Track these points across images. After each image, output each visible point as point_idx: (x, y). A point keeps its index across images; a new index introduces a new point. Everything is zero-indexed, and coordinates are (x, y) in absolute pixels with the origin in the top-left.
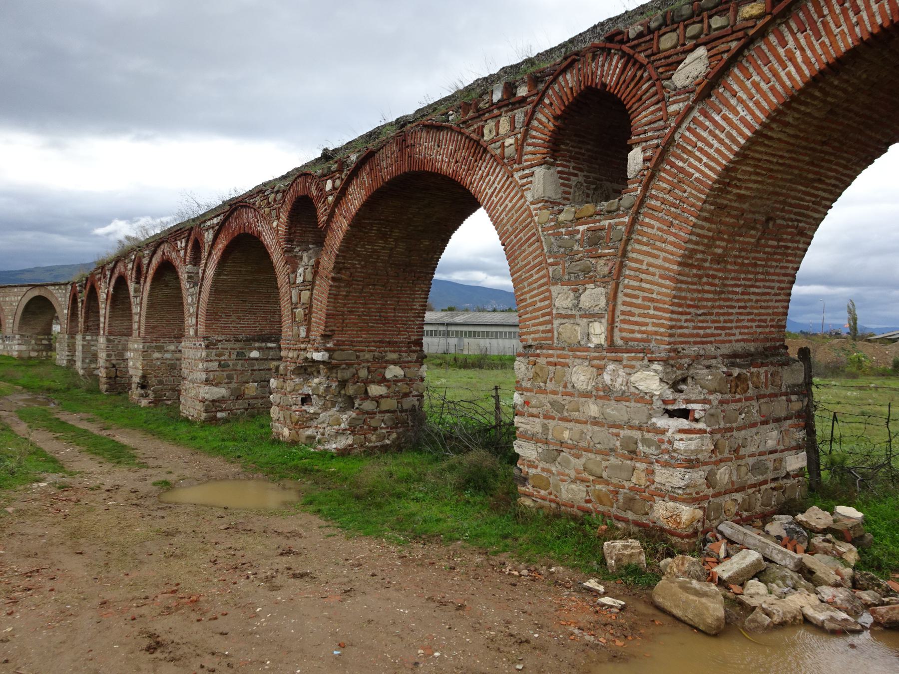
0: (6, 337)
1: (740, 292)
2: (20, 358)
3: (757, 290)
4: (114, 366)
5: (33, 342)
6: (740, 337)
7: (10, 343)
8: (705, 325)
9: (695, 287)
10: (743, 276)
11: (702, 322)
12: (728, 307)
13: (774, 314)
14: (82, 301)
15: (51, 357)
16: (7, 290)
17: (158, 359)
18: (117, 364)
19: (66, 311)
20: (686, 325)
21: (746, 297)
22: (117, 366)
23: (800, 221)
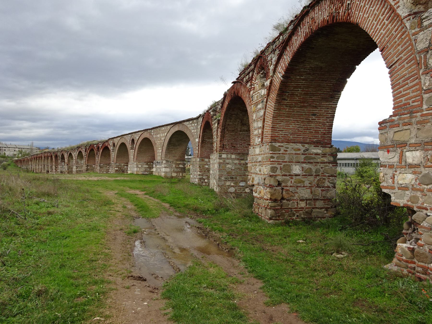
0: (157, 162)
2: (166, 177)
4: (279, 184)
5: (174, 166)
7: (160, 166)
14: (219, 120)
15: (185, 177)
16: (158, 129)
18: (283, 181)
19: (197, 140)
22: (283, 184)
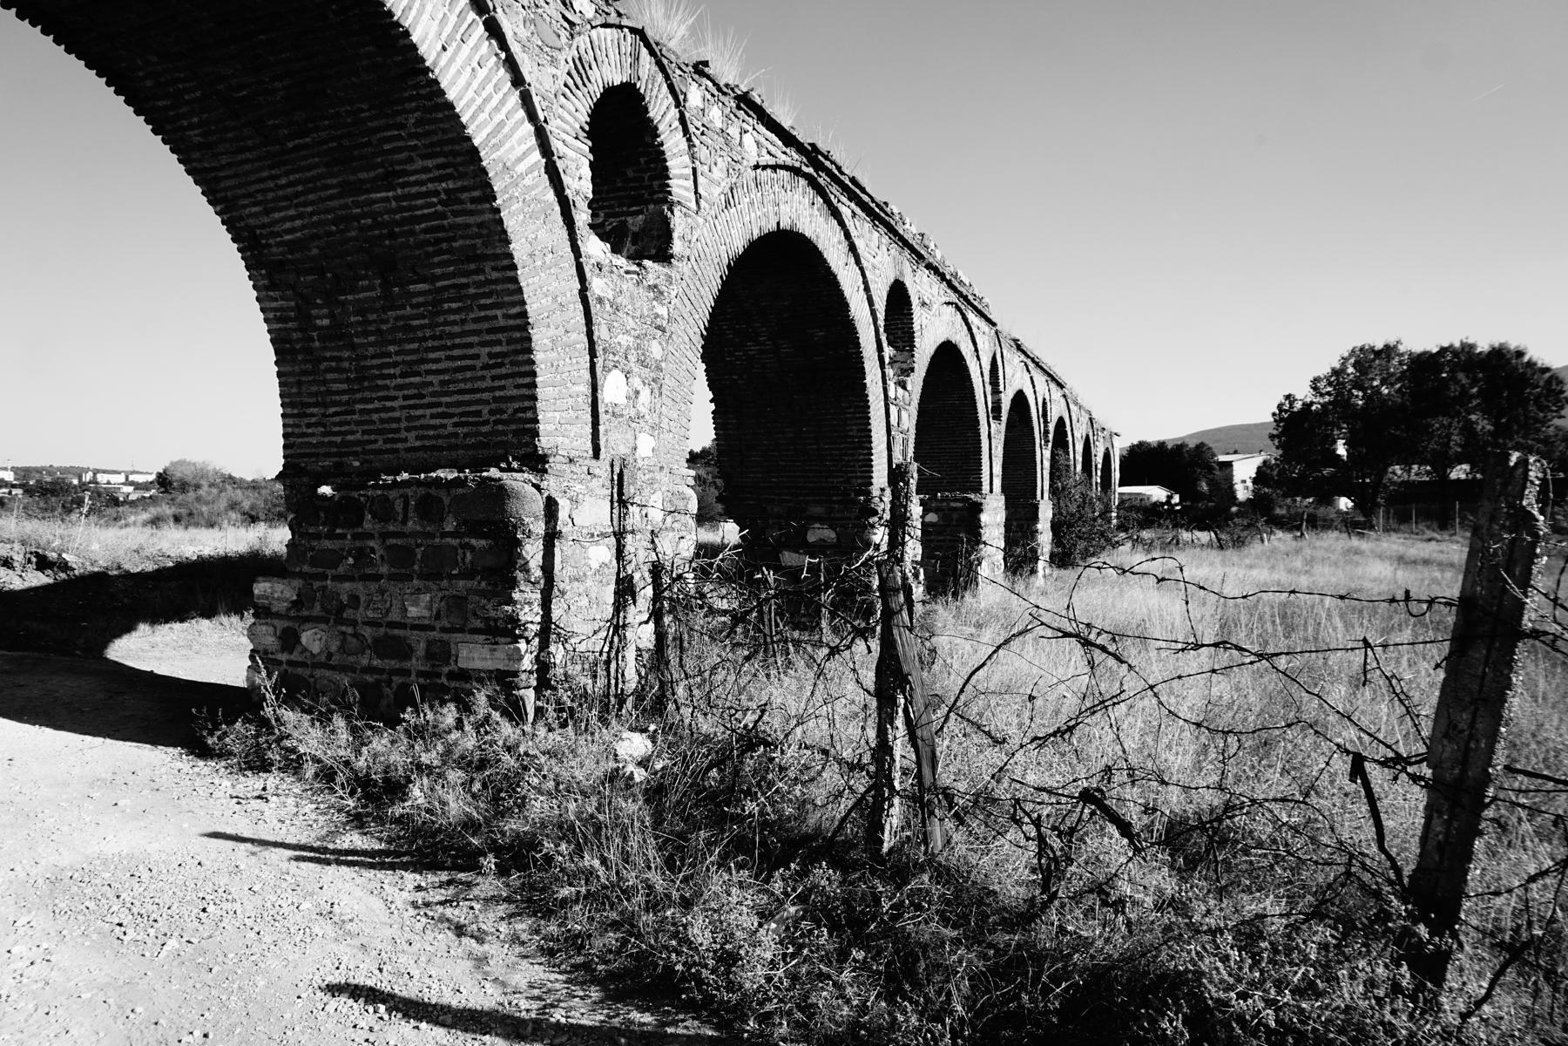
1: (398, 374)
3: (434, 367)
6: (418, 443)
8: (343, 429)
9: (310, 378)
10: (392, 349)
11: (341, 424)
12: (380, 399)
13: (495, 399)
20: (310, 431)
21: (417, 380)
23: (454, 239)
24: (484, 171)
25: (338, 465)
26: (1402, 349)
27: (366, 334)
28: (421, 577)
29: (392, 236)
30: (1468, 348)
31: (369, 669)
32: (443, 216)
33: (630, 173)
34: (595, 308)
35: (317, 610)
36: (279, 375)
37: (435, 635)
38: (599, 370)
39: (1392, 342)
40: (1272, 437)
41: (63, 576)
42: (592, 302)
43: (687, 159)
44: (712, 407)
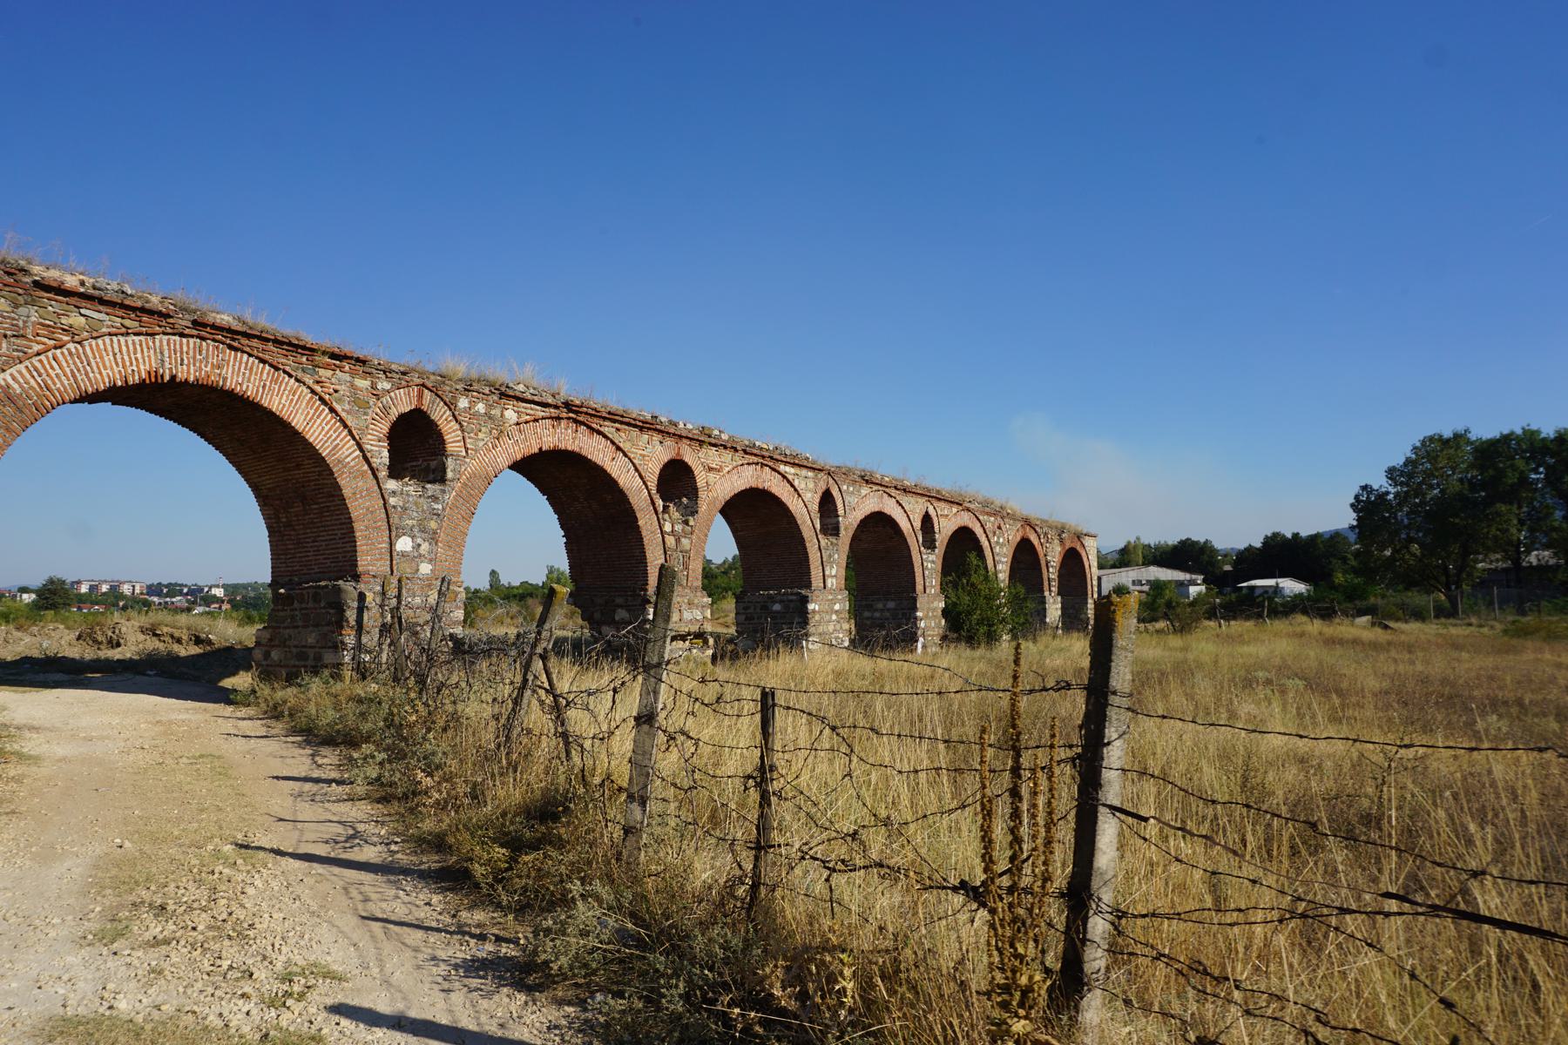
13: (345, 552)
17: (868, 618)
24: (328, 465)
25: (290, 580)
26: (1473, 437)
27: (299, 525)
28: (313, 626)
29: (303, 486)
30: (1530, 436)
31: (294, 666)
32: (318, 480)
33: (431, 442)
34: (391, 510)
35: (277, 642)
36: (270, 541)
37: (317, 650)
38: (393, 538)
39: (1460, 429)
40: (1138, 538)
41: (209, 648)
42: (389, 508)
43: (459, 432)
44: (564, 540)
